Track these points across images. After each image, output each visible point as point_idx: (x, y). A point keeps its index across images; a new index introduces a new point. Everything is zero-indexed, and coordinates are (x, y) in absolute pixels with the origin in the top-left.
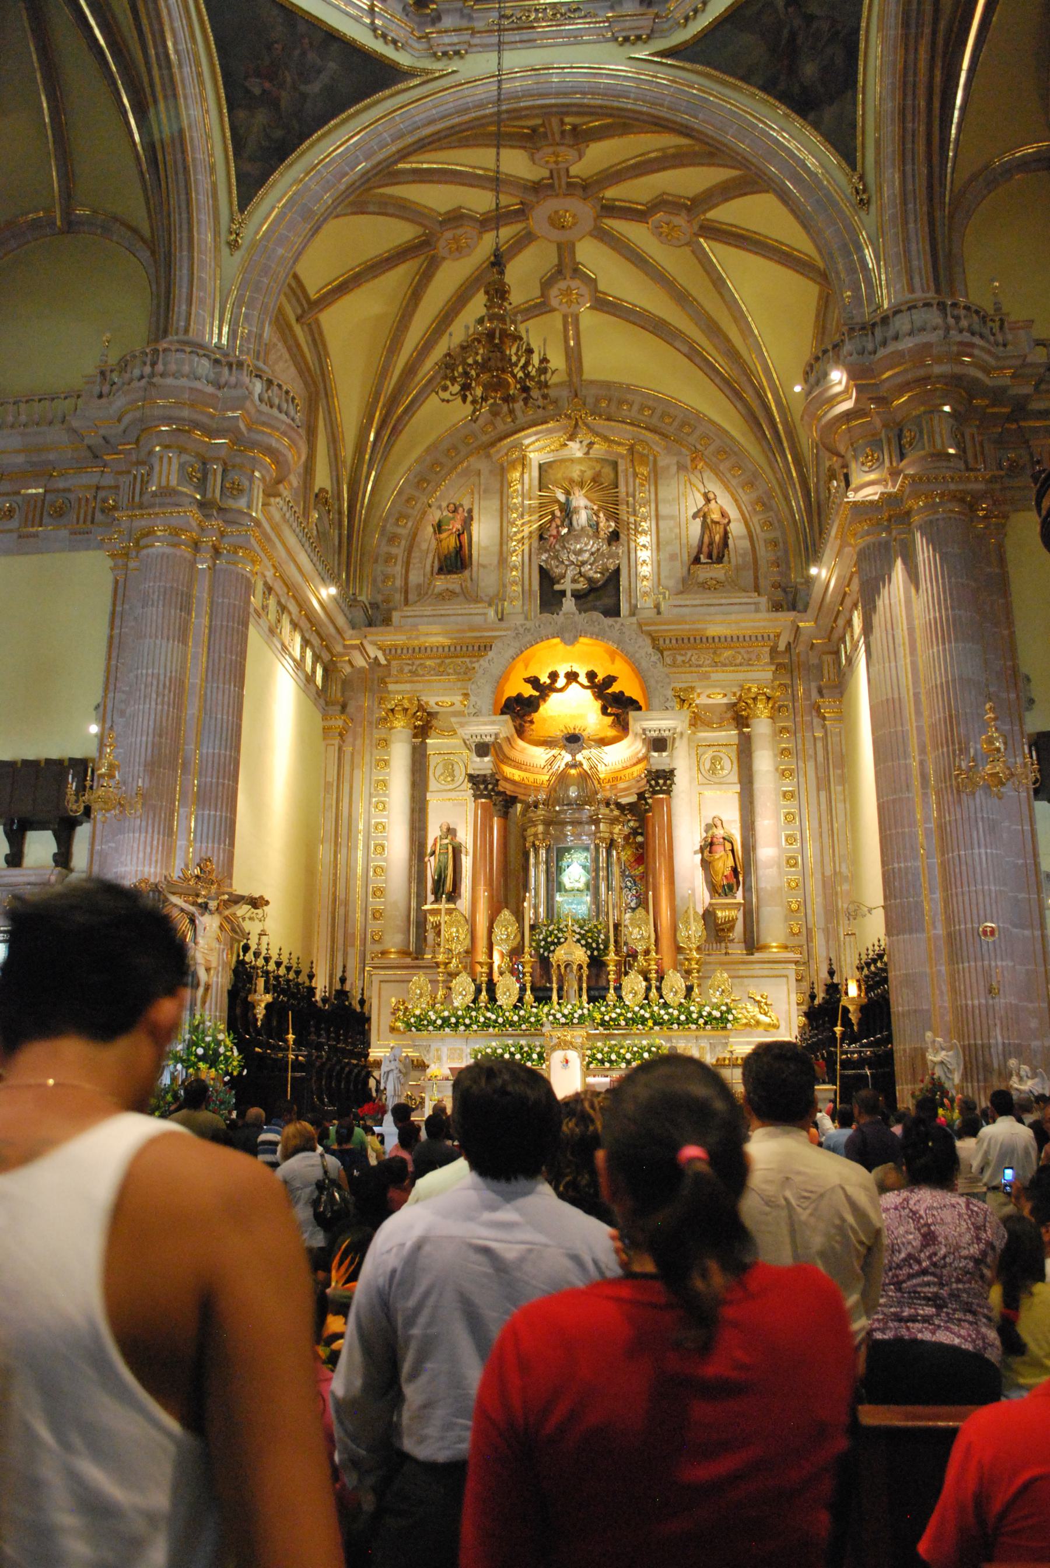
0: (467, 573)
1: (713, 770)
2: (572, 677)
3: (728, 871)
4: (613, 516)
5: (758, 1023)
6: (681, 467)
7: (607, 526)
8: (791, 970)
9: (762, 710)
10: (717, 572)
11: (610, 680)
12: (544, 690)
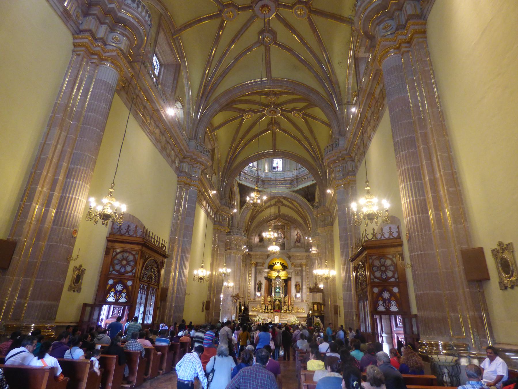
0: (263, 242)
1: (297, 274)
2: (278, 262)
3: (299, 289)
4: (284, 235)
5: (302, 312)
6: (294, 227)
7: (283, 236)
8: (307, 304)
9: (304, 267)
10: (299, 244)
11: (283, 264)
12: (274, 264)
